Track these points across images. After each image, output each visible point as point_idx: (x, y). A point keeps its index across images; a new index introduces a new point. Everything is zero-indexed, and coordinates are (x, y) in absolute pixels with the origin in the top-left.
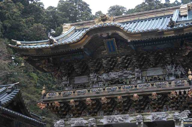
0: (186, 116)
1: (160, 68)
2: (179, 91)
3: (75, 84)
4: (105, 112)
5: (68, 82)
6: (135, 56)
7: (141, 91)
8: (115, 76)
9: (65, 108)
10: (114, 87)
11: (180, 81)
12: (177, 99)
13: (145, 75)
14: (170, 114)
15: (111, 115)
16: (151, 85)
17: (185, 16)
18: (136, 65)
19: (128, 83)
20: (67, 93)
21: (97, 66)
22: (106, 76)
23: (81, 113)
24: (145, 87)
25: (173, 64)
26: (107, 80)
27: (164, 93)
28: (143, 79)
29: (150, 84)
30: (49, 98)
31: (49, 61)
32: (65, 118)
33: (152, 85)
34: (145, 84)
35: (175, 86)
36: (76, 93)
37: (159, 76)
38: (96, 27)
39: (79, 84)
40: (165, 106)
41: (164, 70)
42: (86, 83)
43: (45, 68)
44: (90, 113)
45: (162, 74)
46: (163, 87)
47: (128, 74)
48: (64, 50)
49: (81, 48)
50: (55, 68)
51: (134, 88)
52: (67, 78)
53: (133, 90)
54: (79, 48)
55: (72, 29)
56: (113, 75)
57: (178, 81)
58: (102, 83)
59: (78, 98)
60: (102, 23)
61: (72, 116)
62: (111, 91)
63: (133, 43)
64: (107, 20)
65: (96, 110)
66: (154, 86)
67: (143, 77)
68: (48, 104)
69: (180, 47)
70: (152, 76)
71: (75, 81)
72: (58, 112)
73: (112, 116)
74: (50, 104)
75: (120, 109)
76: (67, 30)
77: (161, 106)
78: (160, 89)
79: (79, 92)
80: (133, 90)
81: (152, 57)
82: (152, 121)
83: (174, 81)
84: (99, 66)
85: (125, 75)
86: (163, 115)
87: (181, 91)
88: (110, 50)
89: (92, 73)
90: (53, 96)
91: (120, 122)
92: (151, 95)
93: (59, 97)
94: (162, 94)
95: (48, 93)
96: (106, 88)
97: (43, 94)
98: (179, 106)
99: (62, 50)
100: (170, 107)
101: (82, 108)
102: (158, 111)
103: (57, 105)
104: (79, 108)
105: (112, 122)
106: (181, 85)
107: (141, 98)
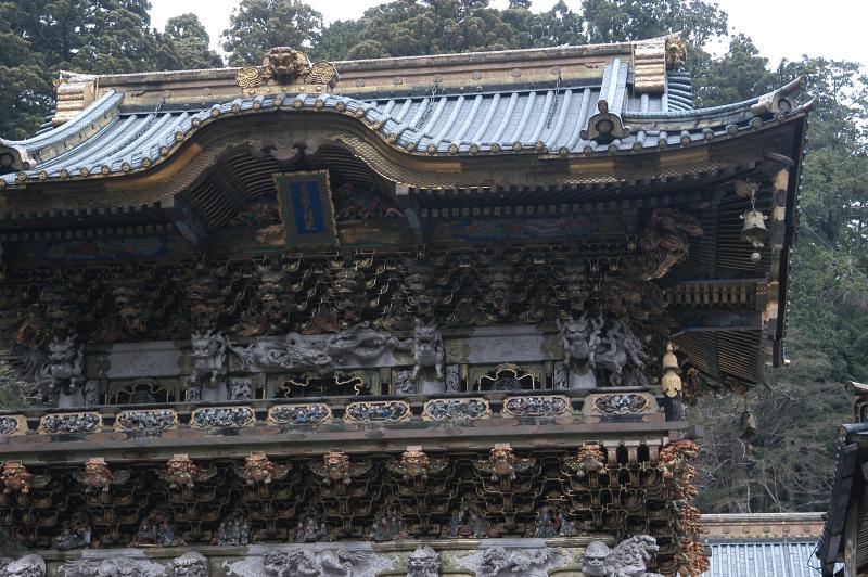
0: (641, 562)
1: (533, 329)
2: (616, 443)
3: (110, 380)
4: (256, 525)
5: (78, 369)
6: (421, 262)
7: (441, 432)
8: (312, 353)
9: (55, 500)
10: (311, 408)
11: (625, 396)
12: (604, 479)
13: (459, 359)
14: (564, 551)
15: (285, 540)
16: (488, 410)
17: (655, 94)
18: (424, 305)
19: (376, 391)
20: (74, 424)
21: (229, 300)
22: (268, 349)
23: (138, 524)
24: (462, 418)
25: (592, 315)
26: (273, 372)
27: (547, 447)
28: (450, 377)
29: (486, 403)
32: (48, 547)
33: (496, 408)
34: (462, 401)
35: (603, 419)
36: (118, 427)
37: (525, 368)
38: (247, 106)
39: (133, 379)
40: (545, 509)
41: (552, 337)
44: (180, 529)
45: (540, 359)
46: (544, 423)
47: (377, 346)
48: (75, 208)
49: (163, 206)
51: (407, 419)
52: (75, 347)
53: (406, 426)
54: (150, 205)
55: (107, 106)
56: (306, 348)
57: (617, 398)
58: (248, 381)
60: (277, 90)
62: (294, 428)
64: (300, 80)
65: (212, 516)
66: (504, 416)
67: (450, 368)
69: (632, 239)
70: (497, 364)
72: (18, 515)
73: (291, 549)
75: (331, 513)
76: (78, 104)
77: (527, 509)
79: (136, 422)
80: (406, 426)
81: (499, 277)
83: (596, 397)
84: (240, 296)
85: (363, 353)
86: (533, 552)
87: (628, 443)
88: (301, 229)
89: (203, 334)
92: (486, 454)
93: (29, 441)
94: (534, 456)
96: (271, 411)
98: (610, 515)
99: (59, 206)
100: (569, 519)
101: (143, 504)
102: (512, 532)
103: (17, 483)
104: (125, 500)
106: (629, 418)
107: (440, 466)
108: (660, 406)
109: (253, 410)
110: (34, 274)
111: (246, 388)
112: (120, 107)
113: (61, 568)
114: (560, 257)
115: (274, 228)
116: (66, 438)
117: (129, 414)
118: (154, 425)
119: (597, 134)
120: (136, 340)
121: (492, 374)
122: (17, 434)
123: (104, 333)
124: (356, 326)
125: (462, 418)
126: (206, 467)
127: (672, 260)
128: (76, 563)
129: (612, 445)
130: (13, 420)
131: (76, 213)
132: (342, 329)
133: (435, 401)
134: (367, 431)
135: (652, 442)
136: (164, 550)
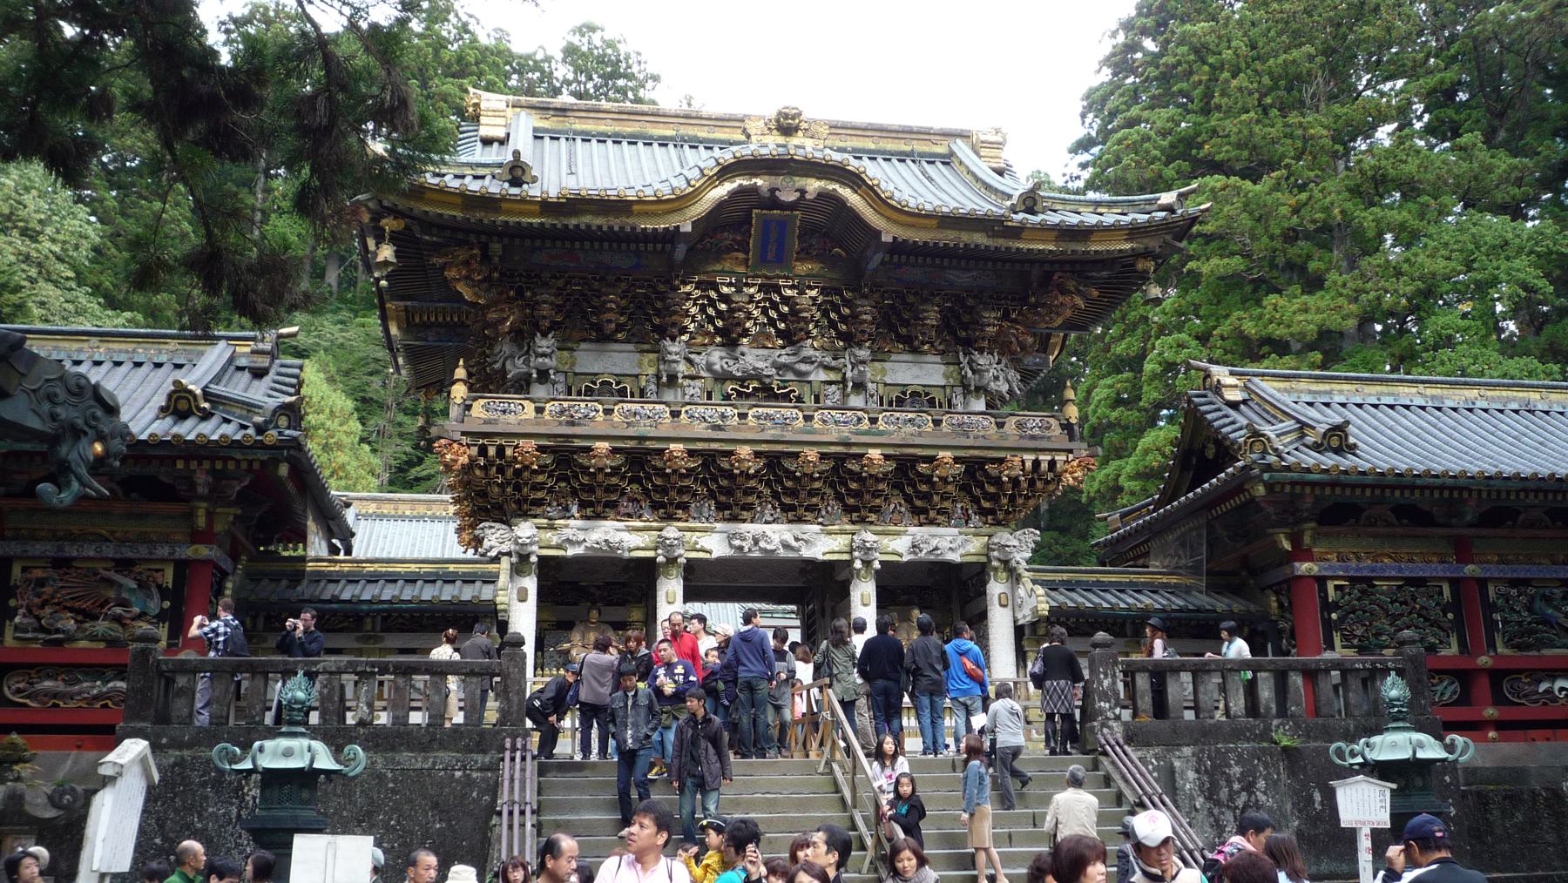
1: (938, 359)
3: (576, 374)
7: (896, 439)
8: (760, 365)
11: (1038, 420)
14: (974, 539)
15: (744, 521)
16: (931, 424)
22: (722, 358)
24: (910, 429)
26: (722, 378)
30: (487, 422)
31: (486, 257)
32: (535, 516)
33: (937, 423)
34: (910, 415)
36: (616, 417)
38: (764, 151)
40: (959, 506)
41: (951, 368)
43: (467, 285)
44: (655, 506)
47: (812, 363)
48: (599, 221)
50: (502, 293)
51: (866, 428)
53: (866, 433)
58: (698, 383)
60: (781, 140)
61: (574, 509)
63: (898, 247)
64: (800, 133)
66: (945, 430)
68: (483, 451)
69: (1033, 294)
71: (579, 360)
72: (518, 488)
74: (492, 451)
75: (787, 500)
78: (969, 442)
80: (866, 433)
82: (905, 559)
83: (1014, 419)
85: (803, 367)
90: (511, 418)
91: (782, 553)
93: (538, 424)
95: (482, 402)
97: (459, 401)
102: (932, 523)
105: (750, 550)
106: (1042, 438)
110: (521, 275)
111: (697, 390)
112: (535, 130)
113: (549, 534)
114: (970, 302)
115: (741, 256)
116: (572, 424)
119: (1023, 208)
120: (598, 341)
123: (568, 331)
127: (1068, 313)
128: (565, 530)
131: (605, 228)
135: (1060, 458)
136: (642, 524)
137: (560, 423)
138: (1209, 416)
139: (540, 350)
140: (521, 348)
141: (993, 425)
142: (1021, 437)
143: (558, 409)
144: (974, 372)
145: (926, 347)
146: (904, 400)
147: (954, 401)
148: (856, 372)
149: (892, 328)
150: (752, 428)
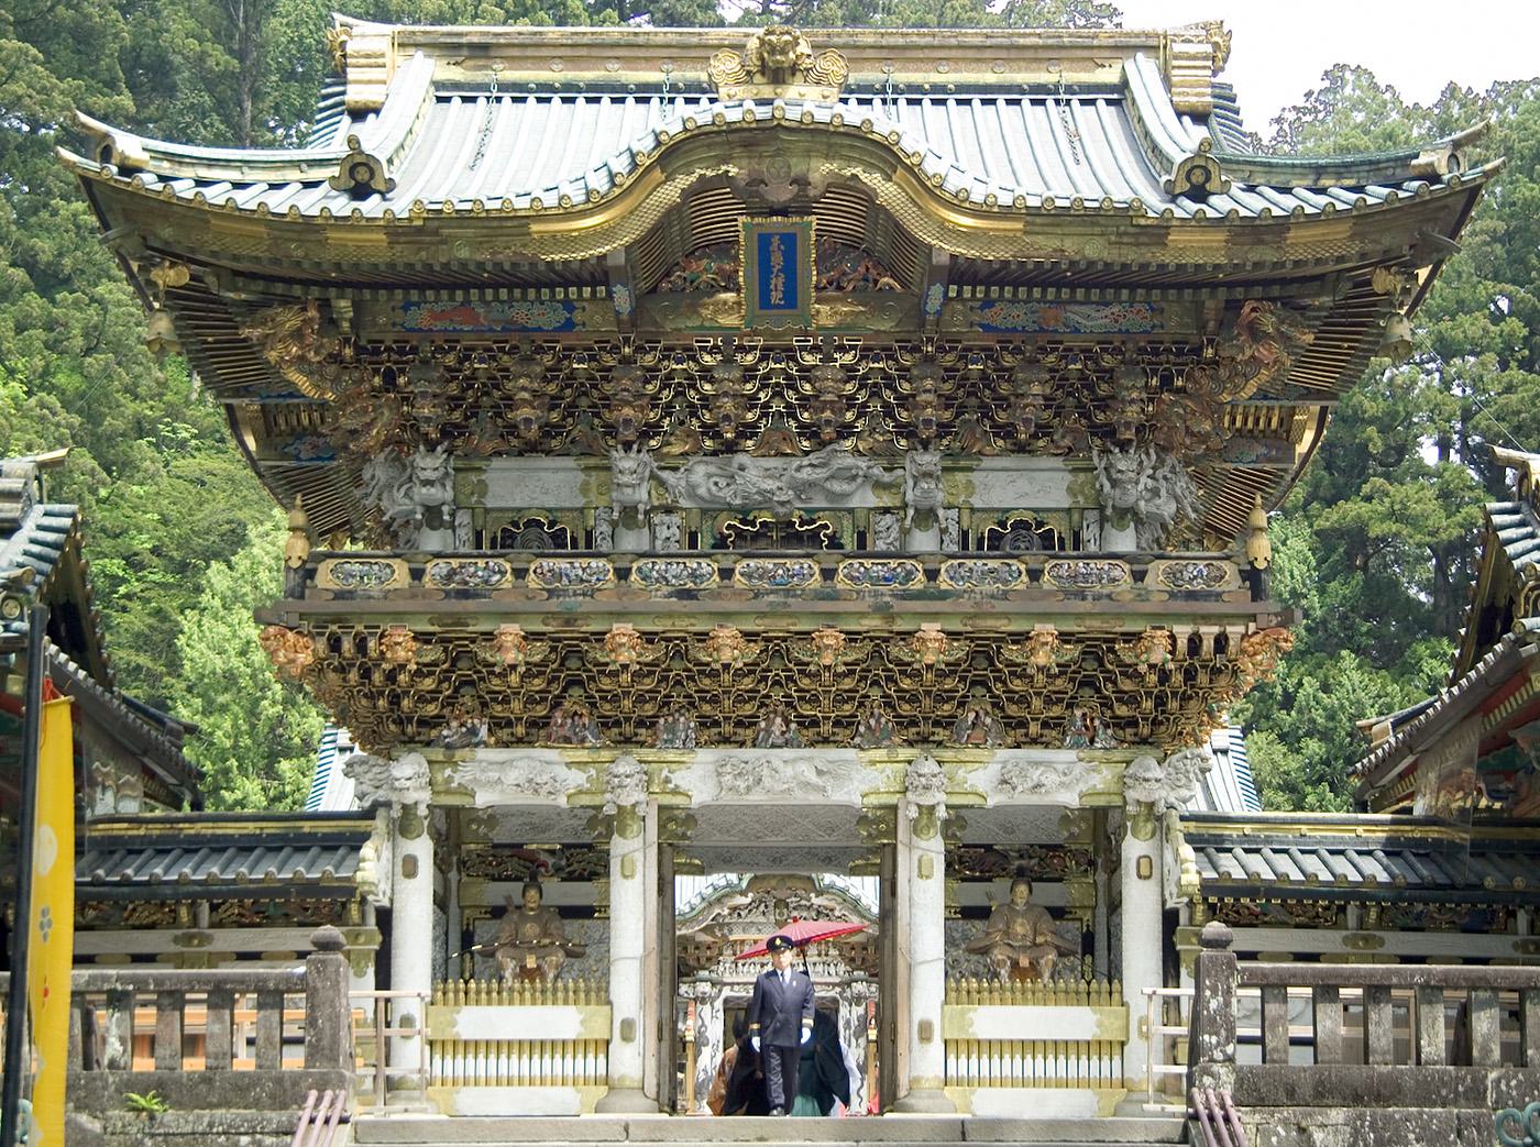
1: (1058, 462)
3: (487, 511)
5: (449, 495)
8: (770, 485)
11: (1201, 564)
16: (1025, 578)
20: (474, 575)
22: (710, 476)
30: (340, 595)
33: (1035, 575)
34: (992, 564)
35: (1172, 595)
36: (532, 581)
39: (519, 510)
41: (1082, 476)
42: (561, 510)
51: (920, 586)
57: (1191, 568)
58: (676, 519)
59: (548, 616)
62: (772, 592)
66: (1046, 587)
83: (1163, 565)
85: (837, 487)
87: (1203, 629)
93: (414, 596)
95: (331, 563)
103: (401, 654)
107: (959, 650)
108: (1244, 581)
109: (715, 566)
116: (464, 594)
117: (547, 563)
118: (582, 581)
121: (1002, 524)
122: (398, 586)
124: (829, 448)
125: (990, 587)
126: (650, 642)
129: (1183, 631)
130: (389, 565)
132: (807, 453)
133: (956, 562)
134: (869, 600)
135: (1234, 630)
137: (448, 594)
138: (1510, 550)
139: (424, 475)
140: (404, 467)
141: (1128, 578)
142: (1172, 595)
143: (445, 572)
144: (1114, 483)
145: (1041, 443)
146: (1002, 536)
147: (1085, 535)
148: (918, 492)
149: (986, 413)
150: (741, 593)
